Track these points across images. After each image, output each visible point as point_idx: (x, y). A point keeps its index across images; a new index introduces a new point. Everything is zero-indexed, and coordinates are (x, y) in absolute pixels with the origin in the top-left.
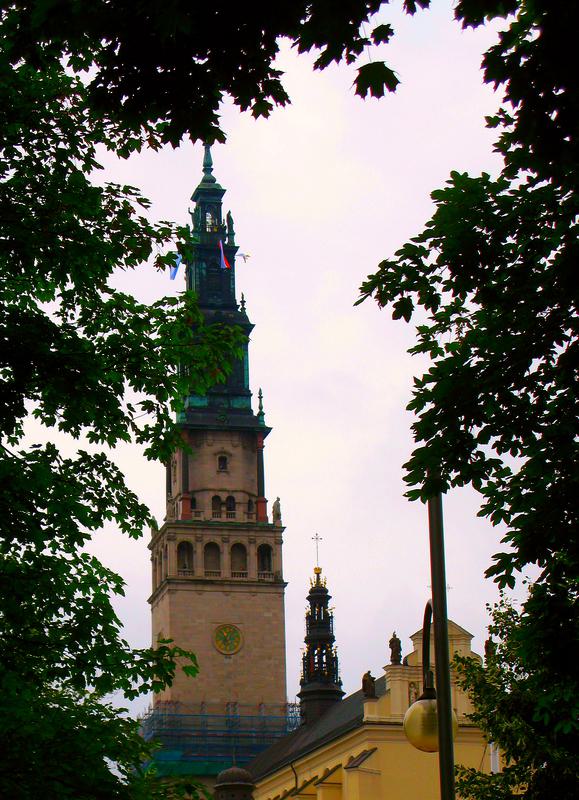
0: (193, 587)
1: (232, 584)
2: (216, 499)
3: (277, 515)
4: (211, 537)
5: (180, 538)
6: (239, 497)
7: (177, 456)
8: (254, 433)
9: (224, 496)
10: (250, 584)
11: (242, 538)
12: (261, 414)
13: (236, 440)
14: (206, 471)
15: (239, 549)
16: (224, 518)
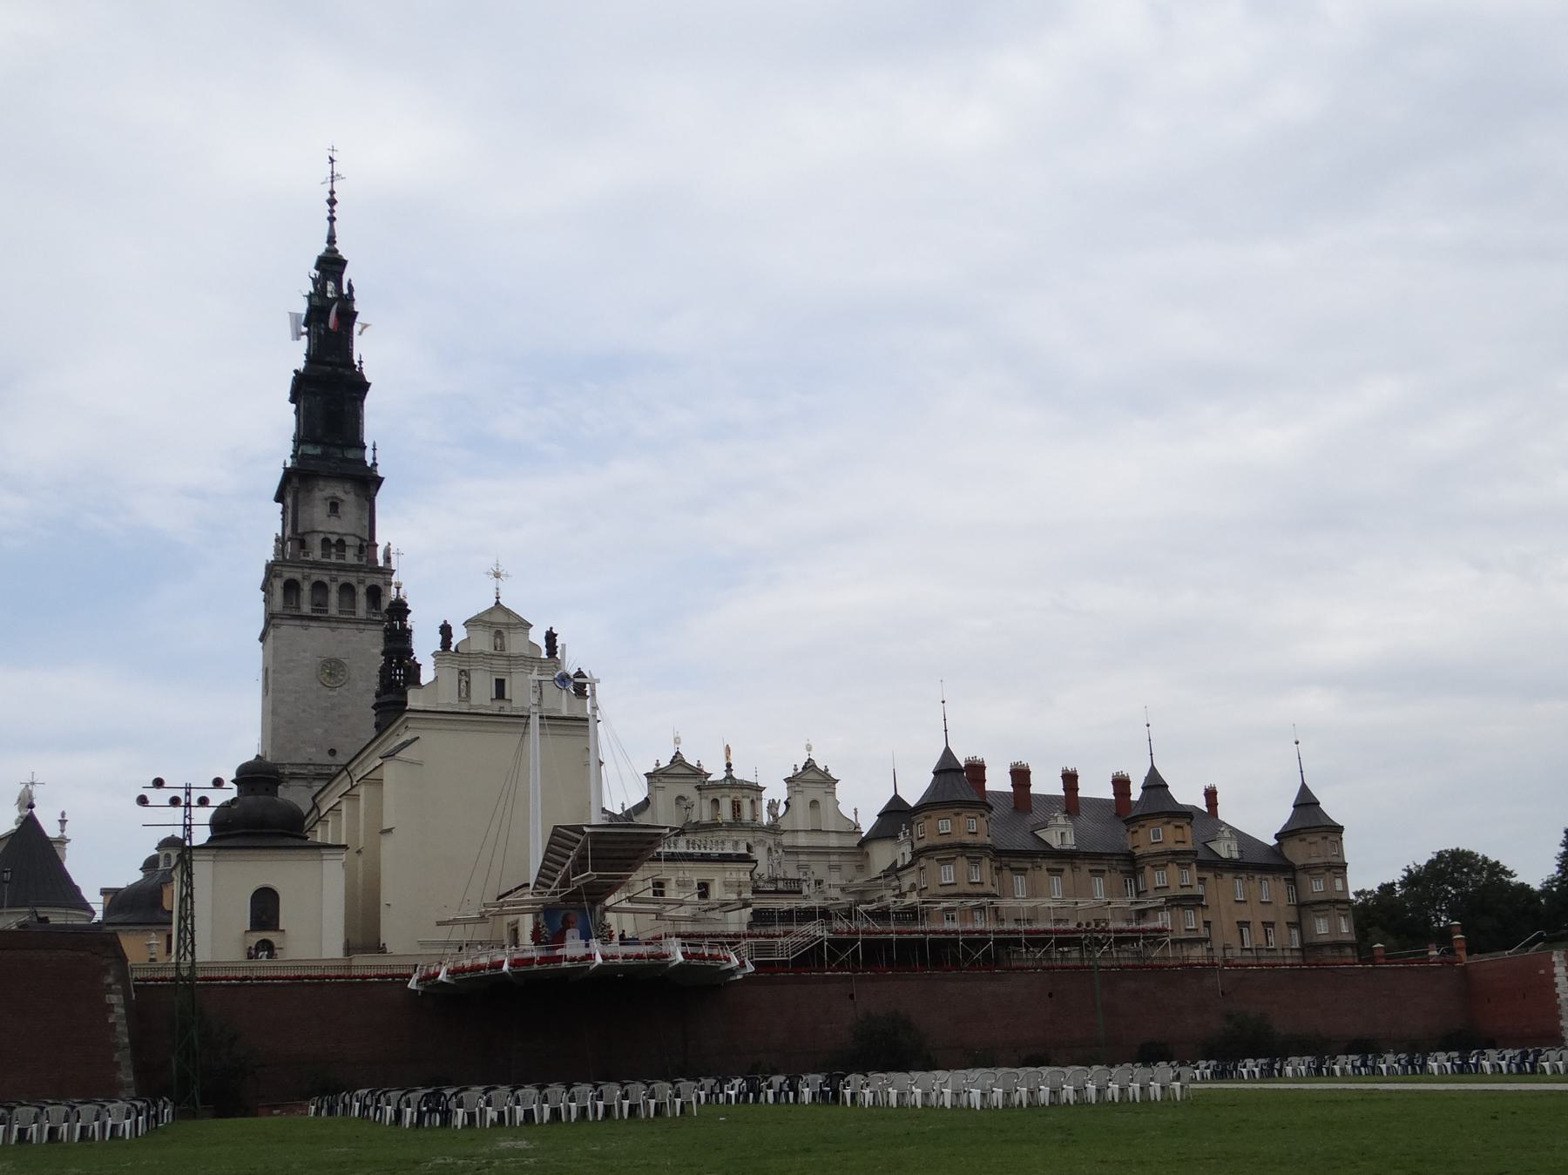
0: (298, 622)
1: (338, 620)
2: (326, 542)
3: (388, 559)
4: (317, 575)
5: (287, 575)
6: (349, 540)
7: (289, 500)
8: (368, 483)
9: (334, 539)
10: (358, 622)
11: (352, 578)
12: (375, 465)
13: (348, 486)
14: (318, 517)
15: (347, 590)
16: (333, 559)
